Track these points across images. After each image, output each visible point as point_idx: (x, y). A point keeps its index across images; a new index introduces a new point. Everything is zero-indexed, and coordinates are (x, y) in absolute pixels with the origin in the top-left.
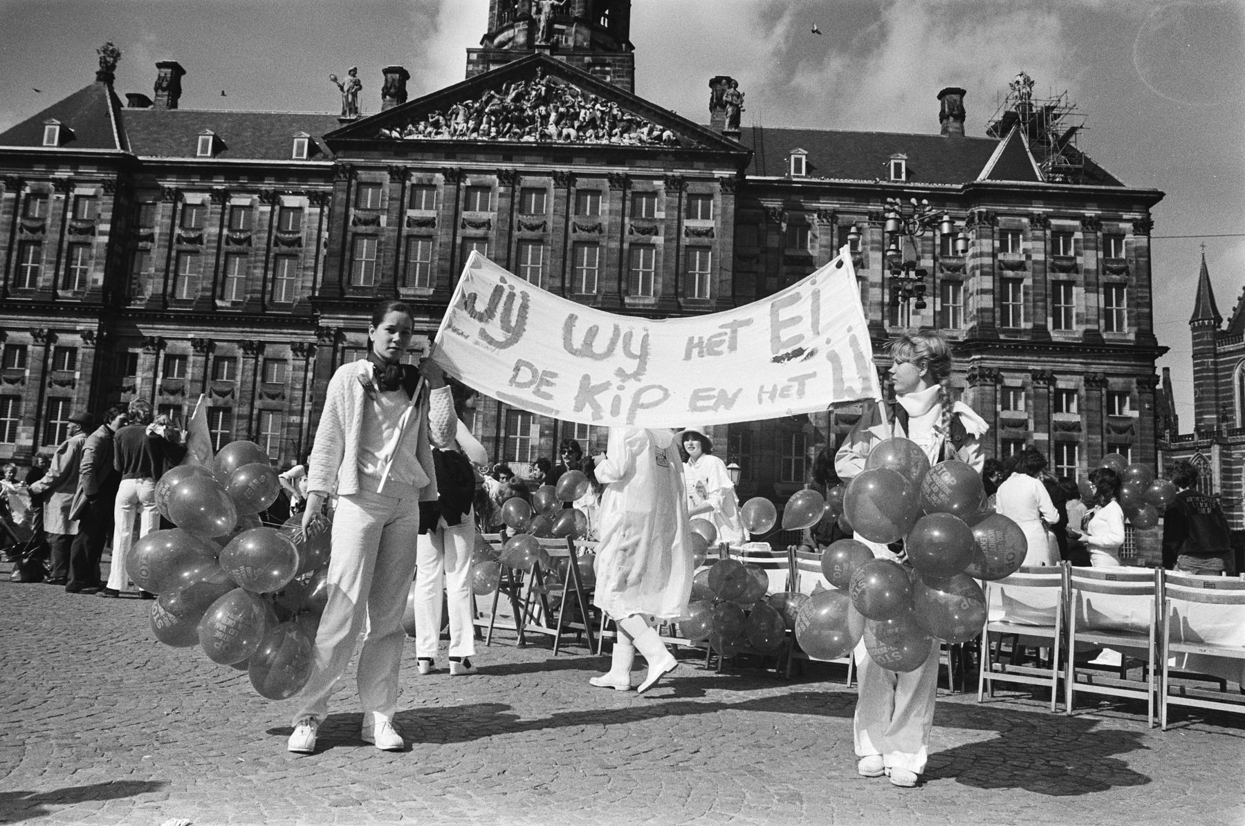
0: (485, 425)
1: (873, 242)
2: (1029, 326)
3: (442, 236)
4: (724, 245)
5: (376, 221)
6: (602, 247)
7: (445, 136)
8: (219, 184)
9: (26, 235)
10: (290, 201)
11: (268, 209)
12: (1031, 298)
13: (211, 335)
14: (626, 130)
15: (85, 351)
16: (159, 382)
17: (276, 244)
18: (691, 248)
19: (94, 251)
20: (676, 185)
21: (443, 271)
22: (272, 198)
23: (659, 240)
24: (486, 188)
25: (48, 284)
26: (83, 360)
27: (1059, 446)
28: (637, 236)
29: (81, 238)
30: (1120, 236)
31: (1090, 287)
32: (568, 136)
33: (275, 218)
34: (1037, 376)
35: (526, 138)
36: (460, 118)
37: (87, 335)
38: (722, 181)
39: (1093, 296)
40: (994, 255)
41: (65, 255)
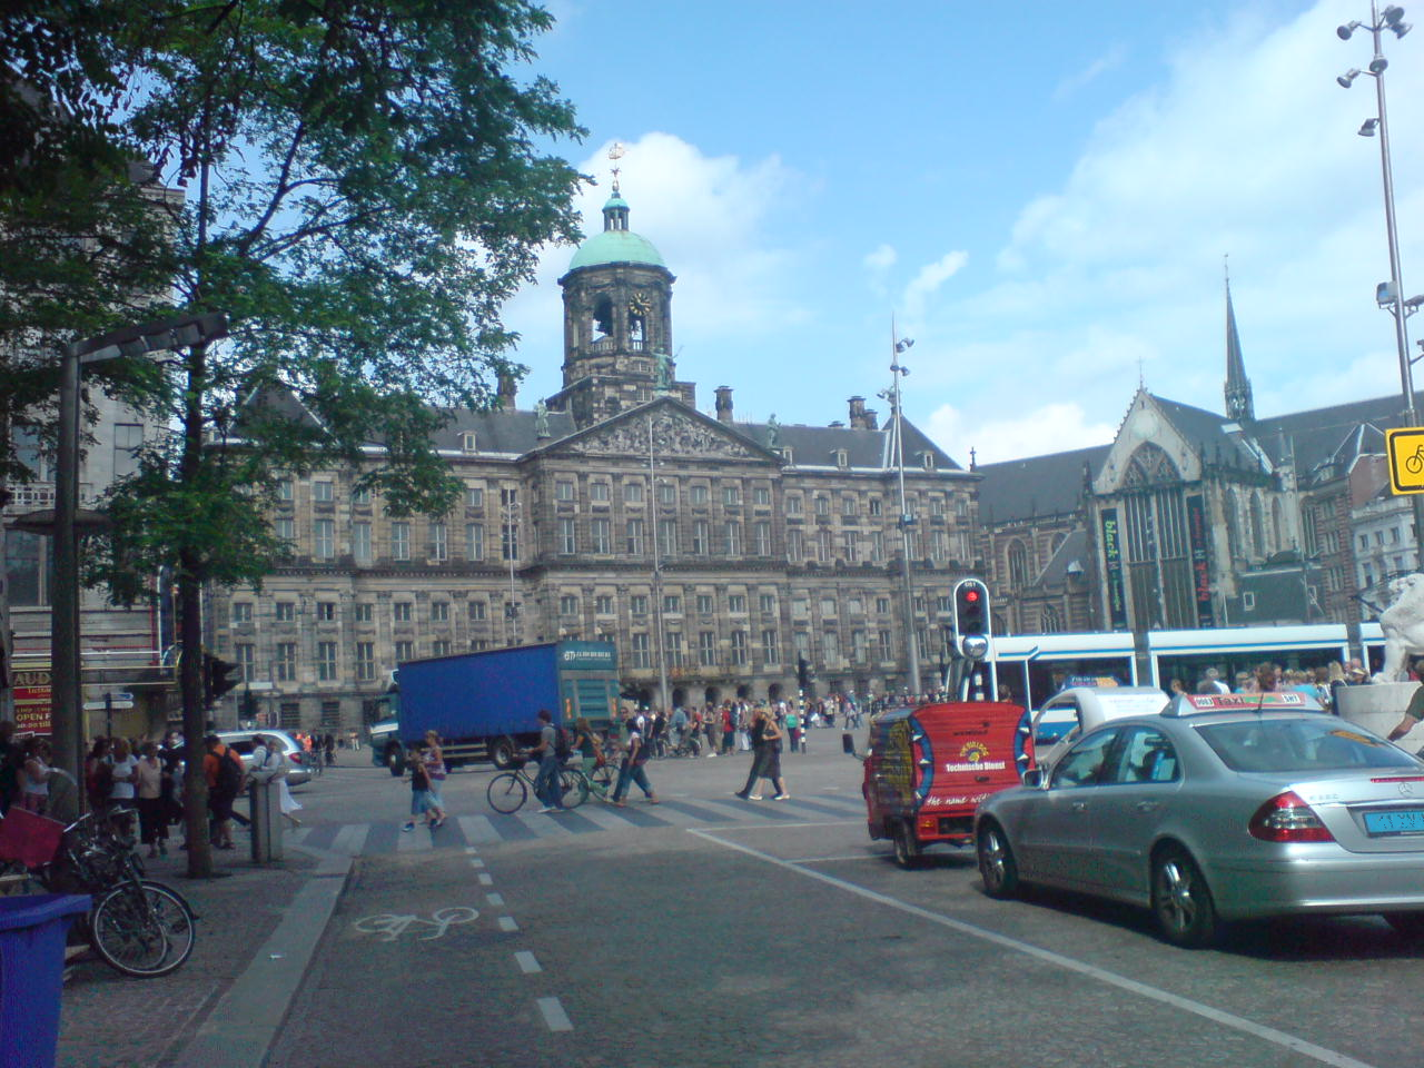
2: (922, 559)
5: (572, 509)
7: (612, 451)
13: (430, 587)
14: (718, 447)
16: (392, 625)
18: (758, 523)
19: (338, 527)
20: (746, 482)
25: (305, 554)
27: (941, 629)
29: (326, 515)
30: (963, 502)
31: (950, 534)
32: (688, 452)
38: (774, 482)
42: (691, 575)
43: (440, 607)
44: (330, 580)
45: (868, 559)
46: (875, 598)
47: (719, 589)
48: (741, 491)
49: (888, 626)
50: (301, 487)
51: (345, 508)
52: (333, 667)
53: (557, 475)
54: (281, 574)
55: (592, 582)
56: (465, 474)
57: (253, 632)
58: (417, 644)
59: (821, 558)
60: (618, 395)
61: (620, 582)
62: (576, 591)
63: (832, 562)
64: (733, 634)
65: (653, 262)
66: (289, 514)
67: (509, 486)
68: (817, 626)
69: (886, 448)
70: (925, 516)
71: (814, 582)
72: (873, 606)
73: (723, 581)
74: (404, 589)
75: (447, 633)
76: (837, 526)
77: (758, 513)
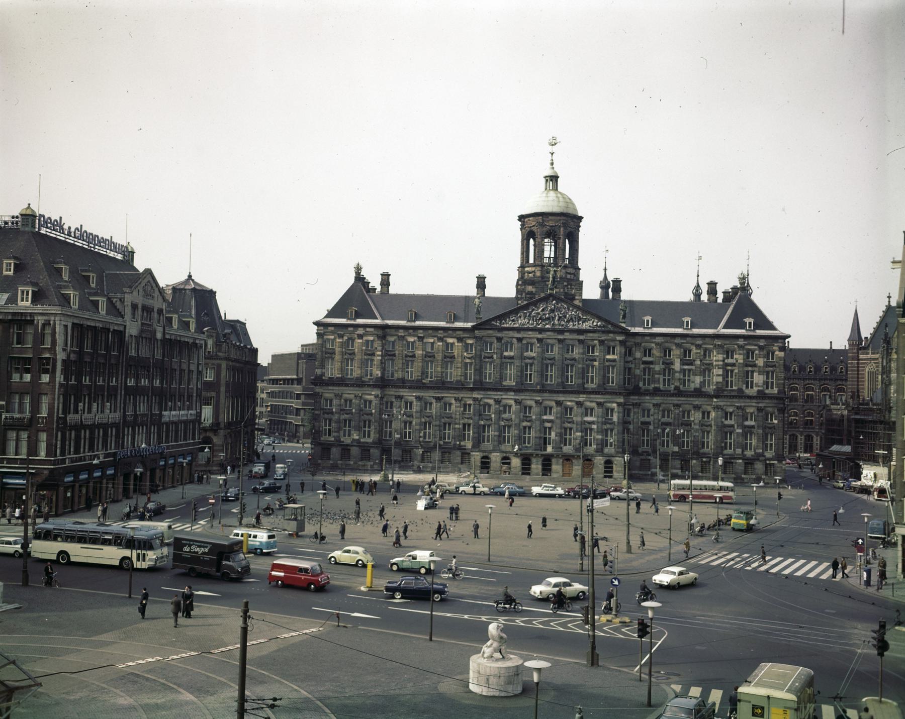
3: (517, 362)
4: (620, 365)
5: (492, 357)
8: (421, 333)
10: (450, 340)
11: (441, 344)
20: (602, 342)
22: (441, 339)
23: (596, 363)
24: (532, 345)
31: (760, 373)
34: (738, 408)
35: (547, 326)
37: (376, 396)
38: (620, 341)
39: (761, 377)
40: (723, 361)
41: (364, 363)
43: (426, 404)
45: (698, 386)
47: (579, 404)
51: (380, 353)
52: (369, 432)
57: (332, 413)
59: (664, 385)
60: (534, 290)
62: (491, 402)
63: (672, 387)
64: (586, 429)
67: (470, 341)
70: (741, 361)
71: (657, 400)
73: (581, 400)
74: (410, 395)
76: (677, 366)
77: (609, 360)
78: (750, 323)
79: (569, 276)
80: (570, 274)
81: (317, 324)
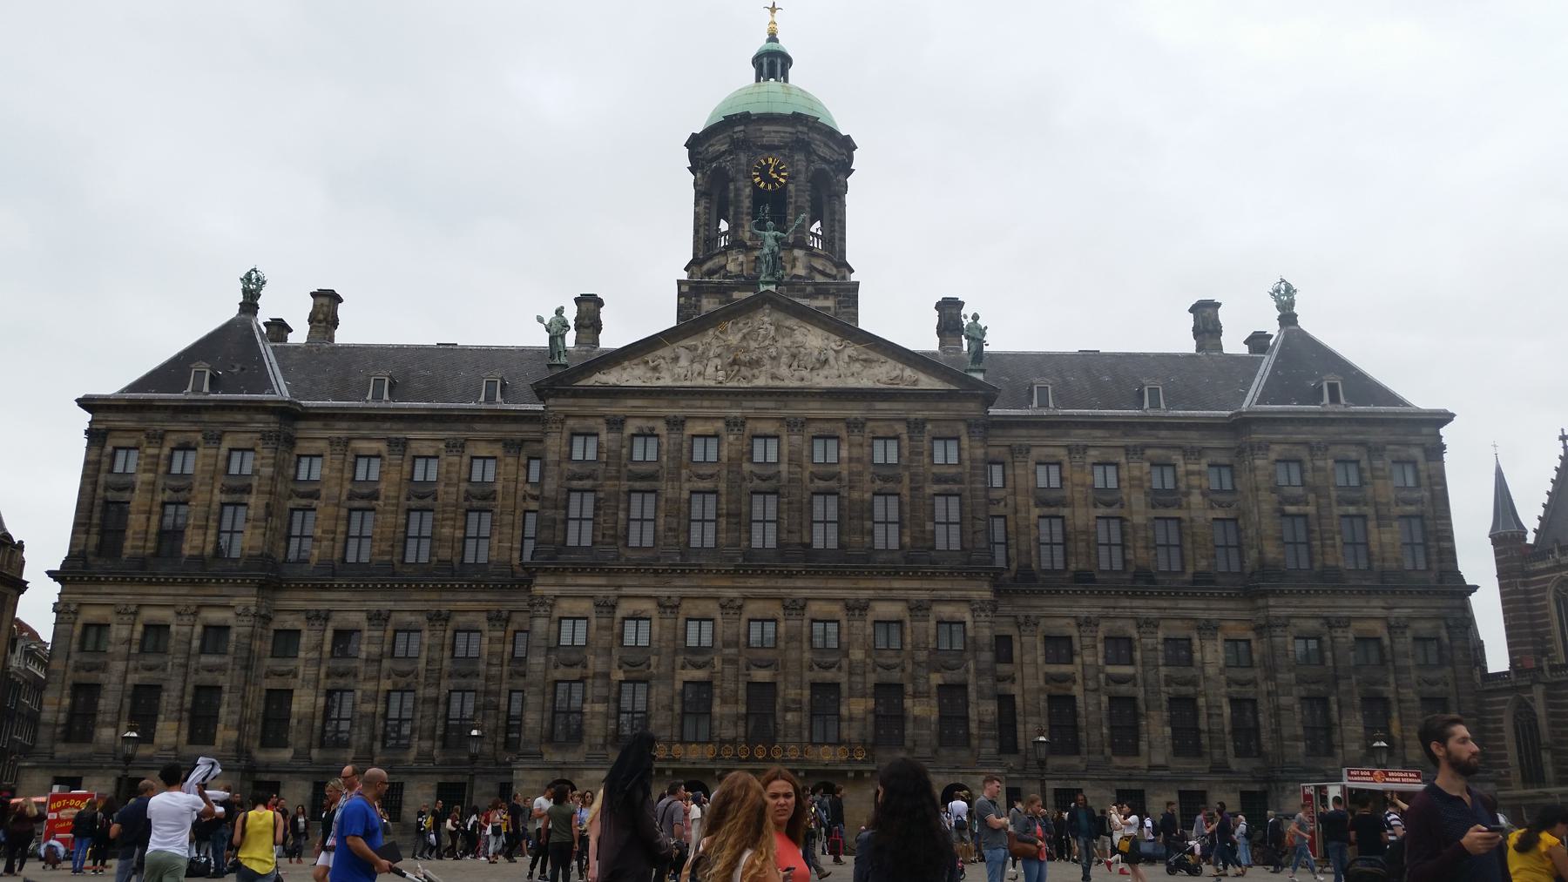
0: (724, 701)
1: (1131, 479)
6: (840, 498)
7: (666, 381)
9: (167, 495)
12: (1317, 535)
13: (390, 605)
15: (240, 629)
17: (466, 499)
19: (251, 513)
21: (670, 530)
25: (195, 552)
26: (238, 641)
28: (878, 484)
29: (236, 497)
33: (465, 469)
36: (684, 362)
42: (799, 583)
44: (225, 591)
46: (1220, 635)
47: (857, 608)
48: (905, 442)
49: (1249, 692)
50: (205, 456)
53: (571, 423)
54: (150, 583)
55: (612, 593)
56: (470, 434)
58: (359, 693)
61: (663, 592)
65: (789, 112)
66: (181, 496)
68: (1091, 684)
69: (1257, 380)
71: (1086, 607)
72: (1212, 654)
74: (351, 610)
75: (410, 679)
77: (938, 479)
78: (1333, 389)
79: (819, 279)
80: (823, 273)
81: (86, 403)
